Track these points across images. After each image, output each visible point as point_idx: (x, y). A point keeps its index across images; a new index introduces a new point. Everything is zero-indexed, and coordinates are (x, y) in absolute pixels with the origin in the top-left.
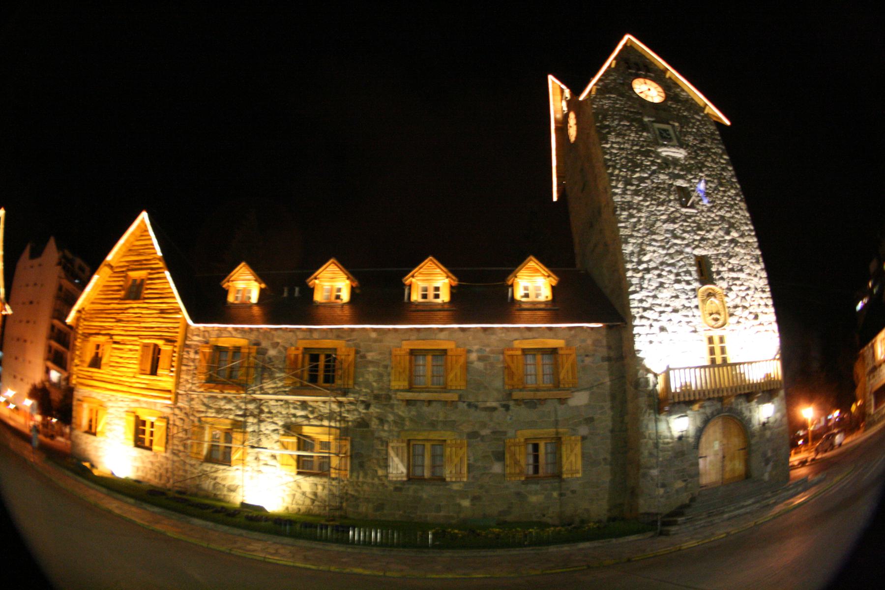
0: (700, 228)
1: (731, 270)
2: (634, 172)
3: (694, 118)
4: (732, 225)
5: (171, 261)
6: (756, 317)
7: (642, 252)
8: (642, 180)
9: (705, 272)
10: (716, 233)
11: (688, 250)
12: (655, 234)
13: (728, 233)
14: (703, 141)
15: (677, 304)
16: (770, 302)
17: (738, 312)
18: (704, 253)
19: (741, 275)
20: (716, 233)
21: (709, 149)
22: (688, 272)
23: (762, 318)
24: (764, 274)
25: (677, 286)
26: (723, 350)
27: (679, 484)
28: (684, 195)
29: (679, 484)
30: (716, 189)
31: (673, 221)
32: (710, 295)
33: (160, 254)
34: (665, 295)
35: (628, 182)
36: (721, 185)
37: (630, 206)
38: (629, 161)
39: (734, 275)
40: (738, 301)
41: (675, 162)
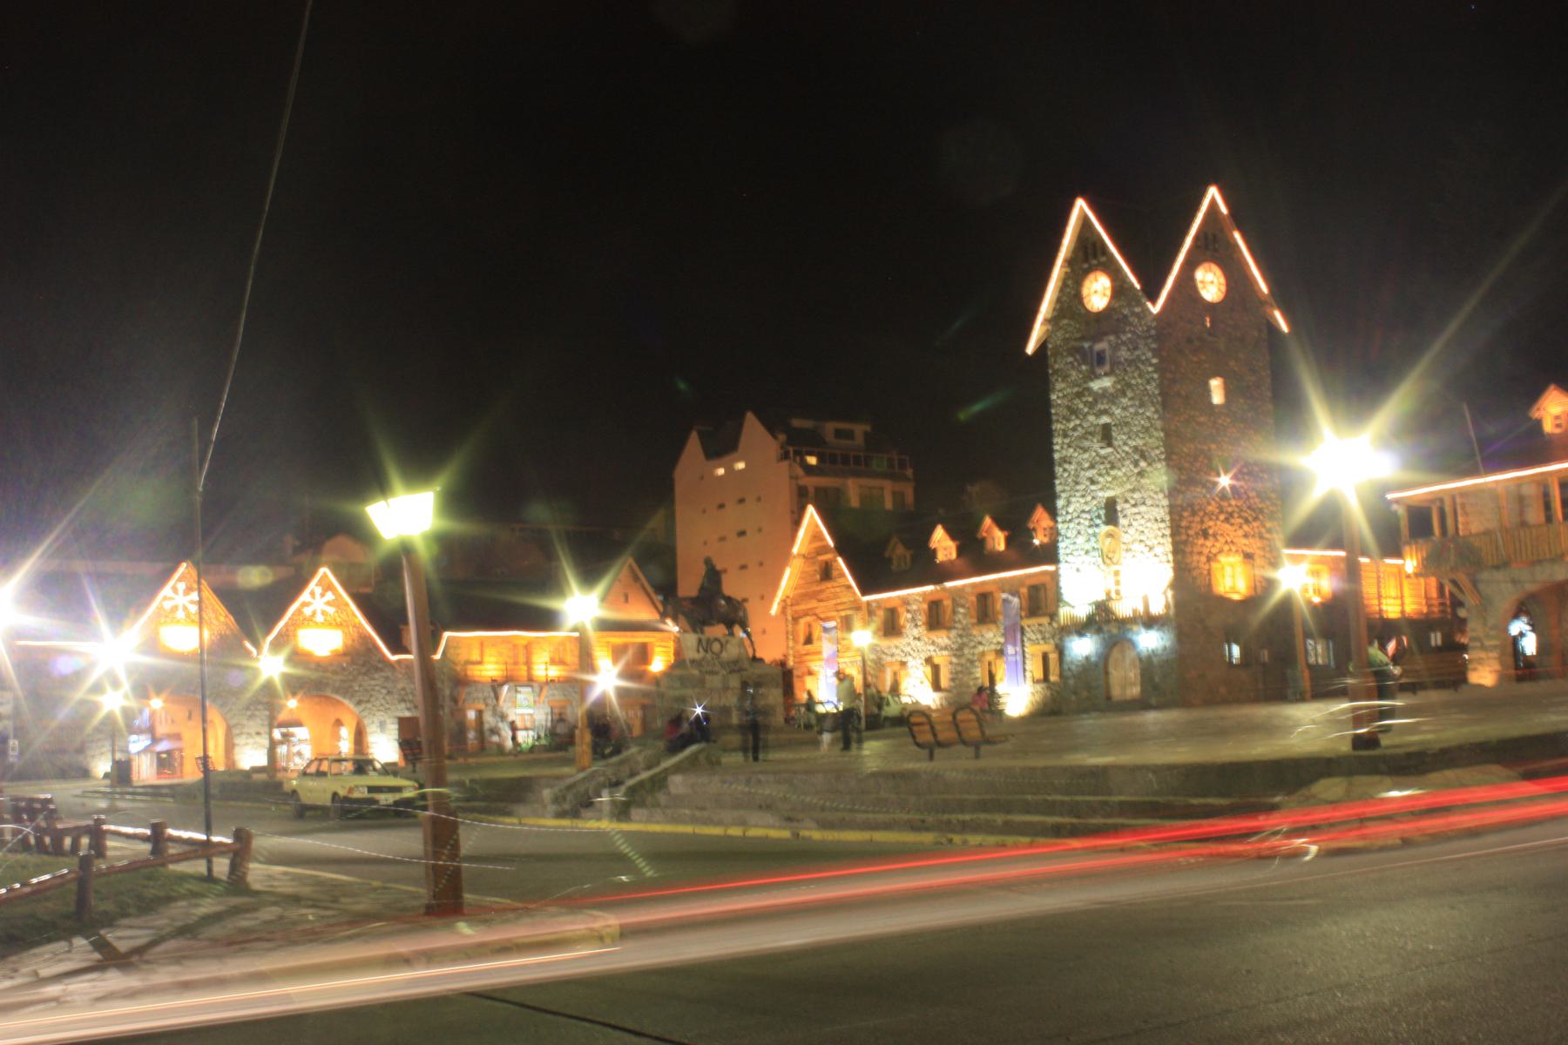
0: (1113, 467)
1: (1134, 506)
2: (1069, 420)
3: (1134, 314)
4: (1143, 456)
5: (841, 549)
6: (1151, 549)
7: (1069, 503)
8: (1074, 429)
9: (1111, 513)
10: (1128, 467)
11: (1100, 494)
12: (1077, 483)
13: (1136, 464)
14: (1136, 348)
15: (1088, 546)
16: (1168, 532)
17: (1137, 547)
18: (1110, 494)
19: (1143, 509)
20: (1128, 467)
21: (1138, 357)
22: (1099, 517)
23: (1159, 550)
24: (1165, 502)
25: (1091, 531)
26: (1117, 583)
27: (1085, 694)
28: (1106, 435)
29: (1085, 694)
30: (1137, 414)
31: (1092, 467)
32: (1110, 535)
33: (831, 543)
34: (1081, 540)
35: (1065, 436)
36: (1142, 405)
37: (1065, 460)
38: (1068, 408)
39: (1135, 510)
40: (1137, 536)
41: (1104, 395)
